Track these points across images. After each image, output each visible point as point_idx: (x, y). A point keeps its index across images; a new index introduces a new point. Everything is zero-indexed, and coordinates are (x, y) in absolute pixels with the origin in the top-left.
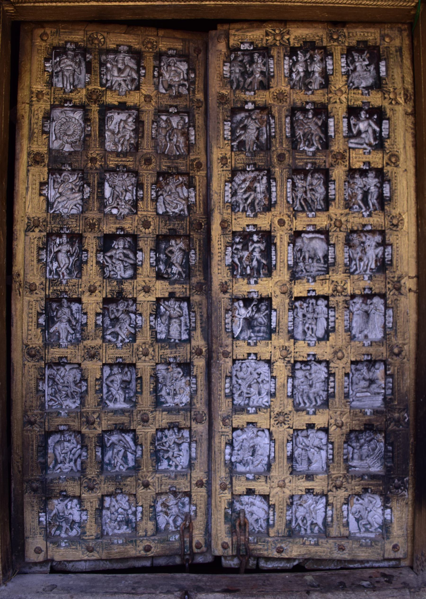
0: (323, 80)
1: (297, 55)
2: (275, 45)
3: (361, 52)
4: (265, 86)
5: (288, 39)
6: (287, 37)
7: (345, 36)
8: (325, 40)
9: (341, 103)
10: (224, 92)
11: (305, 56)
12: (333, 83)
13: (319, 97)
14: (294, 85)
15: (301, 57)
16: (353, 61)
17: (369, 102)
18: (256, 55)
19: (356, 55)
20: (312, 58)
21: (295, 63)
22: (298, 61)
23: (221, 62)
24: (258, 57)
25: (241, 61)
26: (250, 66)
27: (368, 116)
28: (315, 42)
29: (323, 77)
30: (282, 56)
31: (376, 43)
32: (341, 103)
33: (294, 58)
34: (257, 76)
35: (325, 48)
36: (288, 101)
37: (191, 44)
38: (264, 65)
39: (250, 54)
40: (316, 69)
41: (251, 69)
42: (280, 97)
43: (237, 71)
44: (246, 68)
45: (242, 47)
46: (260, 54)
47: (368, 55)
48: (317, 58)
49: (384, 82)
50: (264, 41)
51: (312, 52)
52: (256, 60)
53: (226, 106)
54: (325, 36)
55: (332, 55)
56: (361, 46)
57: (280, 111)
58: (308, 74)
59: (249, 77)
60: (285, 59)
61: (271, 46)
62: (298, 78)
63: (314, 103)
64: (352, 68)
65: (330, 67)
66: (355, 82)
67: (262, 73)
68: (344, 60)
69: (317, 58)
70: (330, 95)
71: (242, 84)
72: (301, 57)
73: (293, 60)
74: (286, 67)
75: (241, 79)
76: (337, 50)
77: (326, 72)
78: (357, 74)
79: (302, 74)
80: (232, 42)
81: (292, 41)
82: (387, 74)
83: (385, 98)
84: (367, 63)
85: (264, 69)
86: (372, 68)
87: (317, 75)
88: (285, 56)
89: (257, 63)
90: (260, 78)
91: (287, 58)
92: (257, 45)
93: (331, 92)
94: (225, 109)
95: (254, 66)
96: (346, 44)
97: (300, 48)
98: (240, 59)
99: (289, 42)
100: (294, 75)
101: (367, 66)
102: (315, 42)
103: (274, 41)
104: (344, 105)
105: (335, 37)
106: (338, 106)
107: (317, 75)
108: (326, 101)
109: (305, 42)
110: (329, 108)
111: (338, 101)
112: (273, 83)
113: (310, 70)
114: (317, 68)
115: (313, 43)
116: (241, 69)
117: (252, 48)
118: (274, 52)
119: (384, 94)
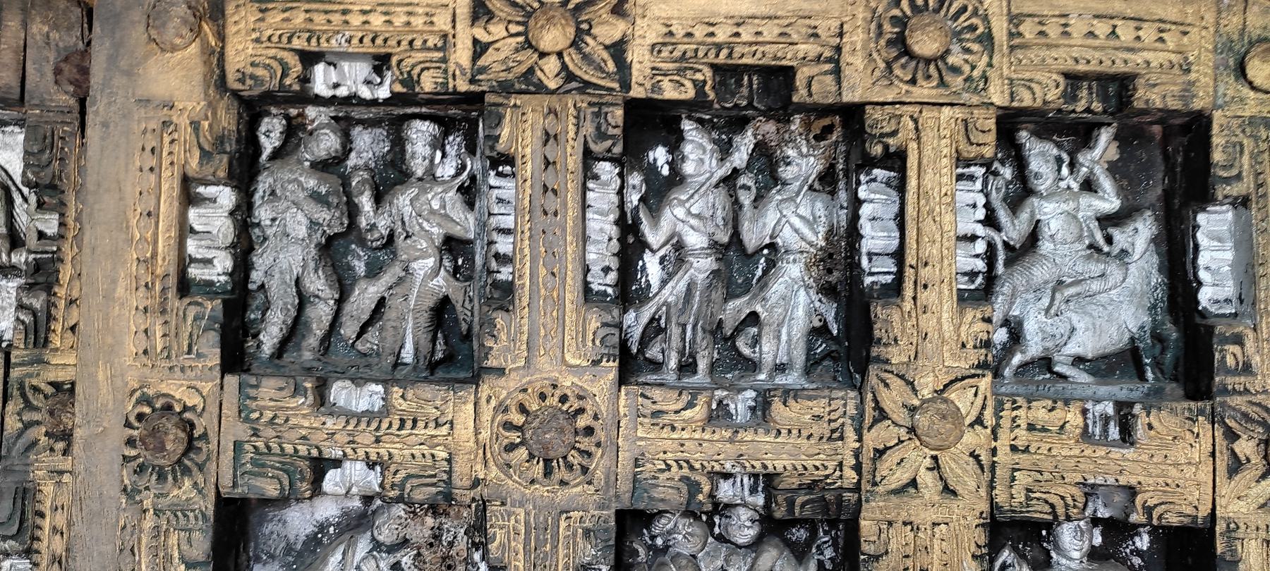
0: (830, 311)
1: (675, 142)
2: (530, 84)
3: (1078, 134)
4: (454, 352)
5: (618, 49)
6: (610, 30)
7: (987, 40)
8: (854, 63)
9: (948, 491)
10: (178, 391)
11: (725, 150)
12: (897, 356)
13: (801, 441)
14: (654, 329)
15: (698, 154)
16: (1022, 191)
17: (1132, 491)
18: (420, 134)
19: (1041, 156)
20: (767, 163)
21: (661, 189)
22: (677, 178)
23: (170, 187)
24: (438, 144)
25: (329, 166)
26: (378, 199)
27: (1098, 540)
28: (787, 73)
29: (828, 291)
30: (574, 161)
31: (1188, 91)
32: (948, 491)
33: (660, 155)
34: (424, 265)
35: (852, 115)
36: (599, 465)
37: (38, 28)
38: (469, 192)
39: (394, 116)
40: (787, 237)
41: (383, 224)
42: (553, 434)
43: (299, 228)
44: (353, 211)
45: (322, 80)
46: (447, 126)
47: (1113, 154)
48: (802, 163)
49: (1230, 355)
50: (462, 55)
51: (770, 128)
52: (419, 168)
53: (184, 491)
54: (856, 38)
55: (896, 160)
56: (1087, 102)
57: (540, 534)
58: (741, 263)
59: (374, 271)
60: (588, 174)
61: (506, 88)
62: (678, 286)
63: (767, 481)
64: (1014, 229)
65: (876, 237)
66: (1031, 327)
67: (453, 246)
68: (970, 194)
69: (802, 163)
70: (874, 438)
71: (321, 314)
72: (698, 154)
73: (650, 172)
74: (603, 226)
75: (317, 284)
76: (935, 140)
77: (853, 266)
78: (1041, 272)
79: (701, 267)
80: (242, 52)
81: (639, 57)
82: (1246, 298)
83: (1236, 466)
84: (1110, 202)
85: (465, 223)
86: (1140, 236)
87: (792, 270)
88: (589, 157)
89: (430, 176)
90: (441, 284)
91: (606, 170)
92: (409, 82)
93: (882, 415)
94: (179, 510)
95: (403, 201)
96: (998, 96)
97: (696, 106)
98: (328, 143)
99: (623, 68)
100: (652, 267)
101: (1107, 221)
102: (787, 73)
103: (528, 58)
104: (969, 511)
105: (925, 43)
106: (926, 507)
107: (792, 270)
108: (850, 475)
109: (727, 74)
110: (867, 526)
111: (927, 479)
112: (504, 343)
113: (752, 238)
114: (794, 221)
115: (778, 79)
116: (323, 215)
117: (383, 93)
118: (520, 130)
119: (1232, 436)
